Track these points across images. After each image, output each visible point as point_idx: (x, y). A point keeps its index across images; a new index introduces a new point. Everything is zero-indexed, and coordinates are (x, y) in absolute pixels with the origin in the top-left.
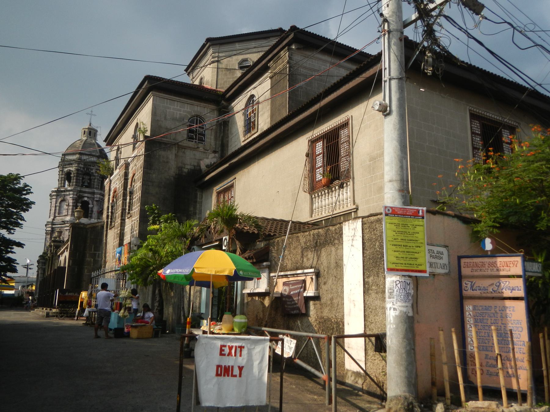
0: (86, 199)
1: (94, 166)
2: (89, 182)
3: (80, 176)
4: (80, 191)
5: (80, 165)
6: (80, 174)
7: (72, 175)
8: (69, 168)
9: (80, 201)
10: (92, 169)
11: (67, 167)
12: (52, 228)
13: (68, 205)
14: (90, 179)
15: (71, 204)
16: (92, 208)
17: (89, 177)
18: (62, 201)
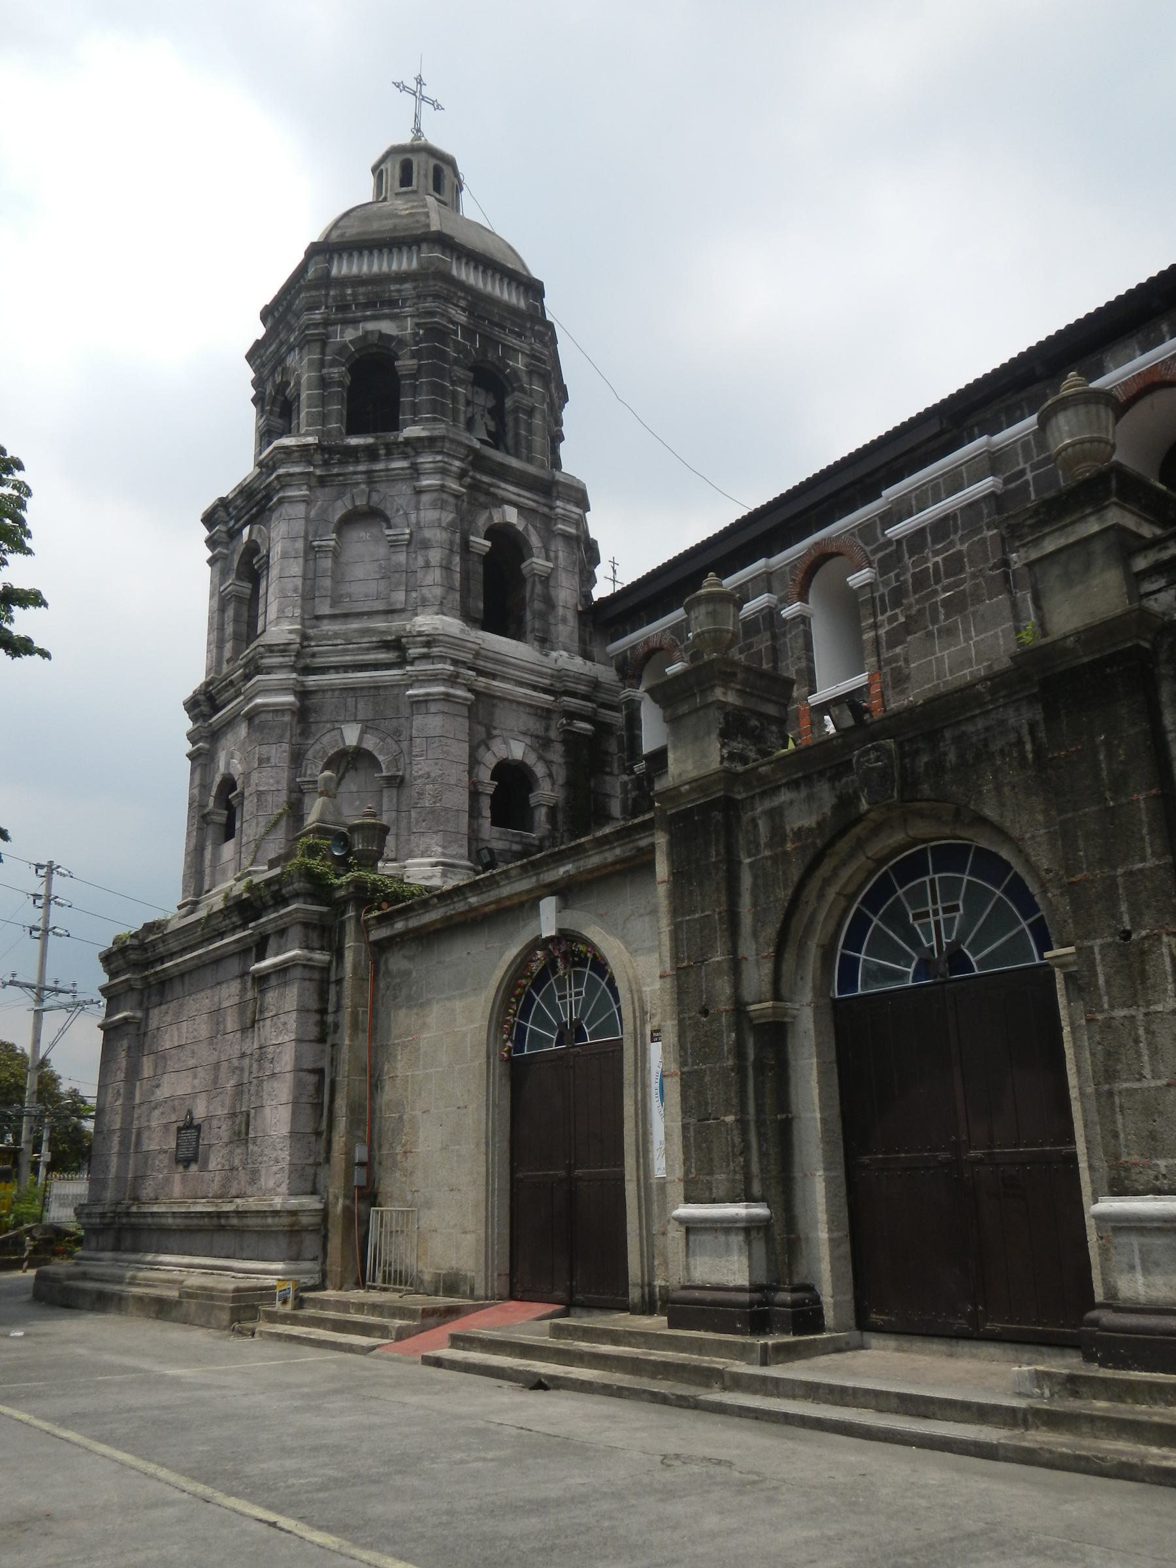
0: (511, 515)
1: (519, 335)
2: (492, 426)
3: (459, 372)
4: (477, 461)
5: (453, 311)
6: (456, 361)
7: (405, 363)
8: (371, 326)
9: (482, 521)
10: (510, 351)
11: (355, 322)
12: (303, 694)
13: (417, 543)
14: (497, 413)
15: (437, 535)
16: (546, 580)
17: (490, 404)
18: (351, 519)
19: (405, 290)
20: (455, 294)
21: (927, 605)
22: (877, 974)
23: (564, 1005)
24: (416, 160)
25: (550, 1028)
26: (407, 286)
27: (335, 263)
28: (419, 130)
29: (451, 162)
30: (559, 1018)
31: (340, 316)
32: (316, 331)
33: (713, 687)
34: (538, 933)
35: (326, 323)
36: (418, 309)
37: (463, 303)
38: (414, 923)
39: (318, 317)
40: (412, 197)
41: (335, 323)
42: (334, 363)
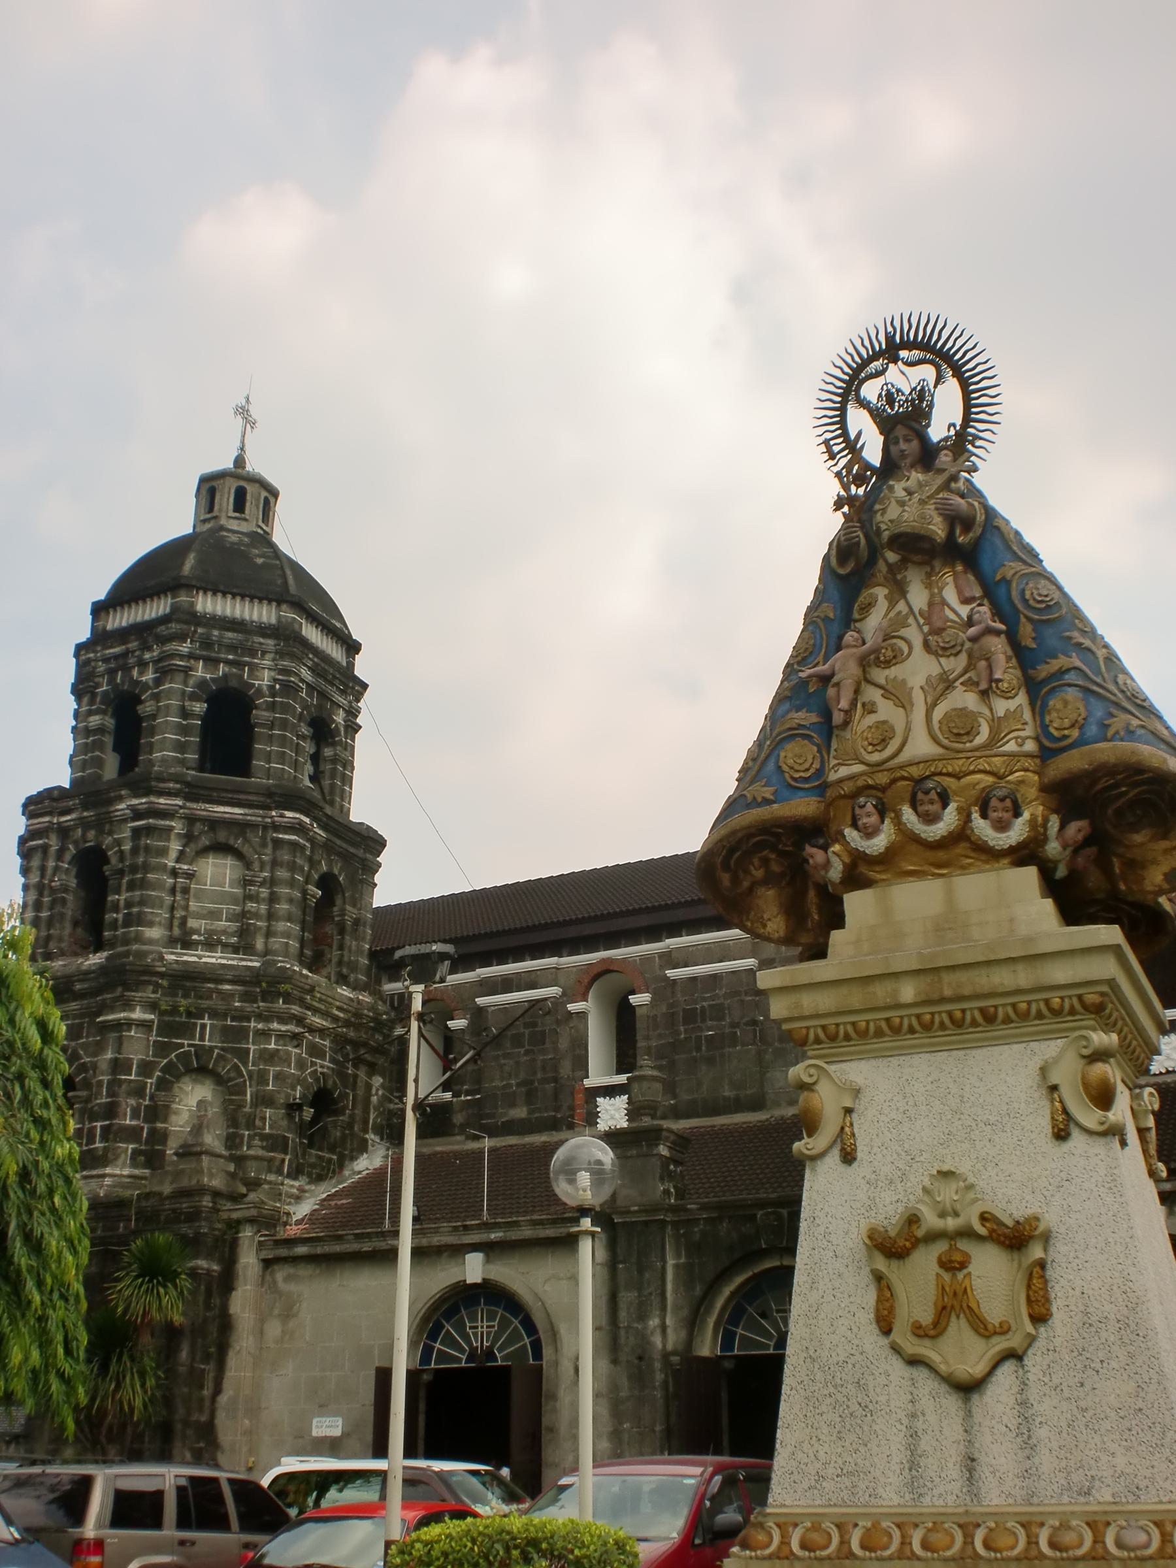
7: (261, 715)
17: (312, 751)
19: (267, 645)
20: (307, 655)
21: (693, 1036)
22: (746, 1342)
23: (475, 1334)
24: (250, 489)
25: (462, 1351)
26: (271, 642)
27: (200, 598)
28: (242, 449)
29: (275, 494)
30: (469, 1343)
31: (204, 653)
32: (181, 663)
33: (657, 1145)
34: (462, 1278)
35: (191, 656)
36: (276, 665)
37: (310, 664)
38: (319, 1251)
39: (186, 650)
40: (244, 523)
41: (197, 658)
42: (193, 697)
